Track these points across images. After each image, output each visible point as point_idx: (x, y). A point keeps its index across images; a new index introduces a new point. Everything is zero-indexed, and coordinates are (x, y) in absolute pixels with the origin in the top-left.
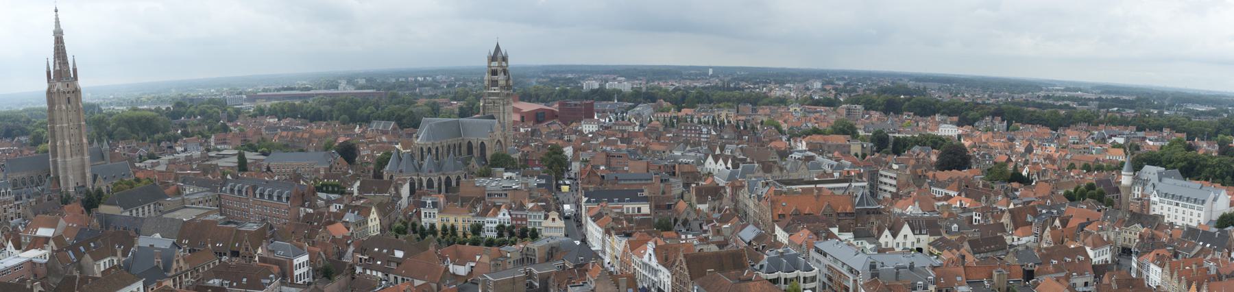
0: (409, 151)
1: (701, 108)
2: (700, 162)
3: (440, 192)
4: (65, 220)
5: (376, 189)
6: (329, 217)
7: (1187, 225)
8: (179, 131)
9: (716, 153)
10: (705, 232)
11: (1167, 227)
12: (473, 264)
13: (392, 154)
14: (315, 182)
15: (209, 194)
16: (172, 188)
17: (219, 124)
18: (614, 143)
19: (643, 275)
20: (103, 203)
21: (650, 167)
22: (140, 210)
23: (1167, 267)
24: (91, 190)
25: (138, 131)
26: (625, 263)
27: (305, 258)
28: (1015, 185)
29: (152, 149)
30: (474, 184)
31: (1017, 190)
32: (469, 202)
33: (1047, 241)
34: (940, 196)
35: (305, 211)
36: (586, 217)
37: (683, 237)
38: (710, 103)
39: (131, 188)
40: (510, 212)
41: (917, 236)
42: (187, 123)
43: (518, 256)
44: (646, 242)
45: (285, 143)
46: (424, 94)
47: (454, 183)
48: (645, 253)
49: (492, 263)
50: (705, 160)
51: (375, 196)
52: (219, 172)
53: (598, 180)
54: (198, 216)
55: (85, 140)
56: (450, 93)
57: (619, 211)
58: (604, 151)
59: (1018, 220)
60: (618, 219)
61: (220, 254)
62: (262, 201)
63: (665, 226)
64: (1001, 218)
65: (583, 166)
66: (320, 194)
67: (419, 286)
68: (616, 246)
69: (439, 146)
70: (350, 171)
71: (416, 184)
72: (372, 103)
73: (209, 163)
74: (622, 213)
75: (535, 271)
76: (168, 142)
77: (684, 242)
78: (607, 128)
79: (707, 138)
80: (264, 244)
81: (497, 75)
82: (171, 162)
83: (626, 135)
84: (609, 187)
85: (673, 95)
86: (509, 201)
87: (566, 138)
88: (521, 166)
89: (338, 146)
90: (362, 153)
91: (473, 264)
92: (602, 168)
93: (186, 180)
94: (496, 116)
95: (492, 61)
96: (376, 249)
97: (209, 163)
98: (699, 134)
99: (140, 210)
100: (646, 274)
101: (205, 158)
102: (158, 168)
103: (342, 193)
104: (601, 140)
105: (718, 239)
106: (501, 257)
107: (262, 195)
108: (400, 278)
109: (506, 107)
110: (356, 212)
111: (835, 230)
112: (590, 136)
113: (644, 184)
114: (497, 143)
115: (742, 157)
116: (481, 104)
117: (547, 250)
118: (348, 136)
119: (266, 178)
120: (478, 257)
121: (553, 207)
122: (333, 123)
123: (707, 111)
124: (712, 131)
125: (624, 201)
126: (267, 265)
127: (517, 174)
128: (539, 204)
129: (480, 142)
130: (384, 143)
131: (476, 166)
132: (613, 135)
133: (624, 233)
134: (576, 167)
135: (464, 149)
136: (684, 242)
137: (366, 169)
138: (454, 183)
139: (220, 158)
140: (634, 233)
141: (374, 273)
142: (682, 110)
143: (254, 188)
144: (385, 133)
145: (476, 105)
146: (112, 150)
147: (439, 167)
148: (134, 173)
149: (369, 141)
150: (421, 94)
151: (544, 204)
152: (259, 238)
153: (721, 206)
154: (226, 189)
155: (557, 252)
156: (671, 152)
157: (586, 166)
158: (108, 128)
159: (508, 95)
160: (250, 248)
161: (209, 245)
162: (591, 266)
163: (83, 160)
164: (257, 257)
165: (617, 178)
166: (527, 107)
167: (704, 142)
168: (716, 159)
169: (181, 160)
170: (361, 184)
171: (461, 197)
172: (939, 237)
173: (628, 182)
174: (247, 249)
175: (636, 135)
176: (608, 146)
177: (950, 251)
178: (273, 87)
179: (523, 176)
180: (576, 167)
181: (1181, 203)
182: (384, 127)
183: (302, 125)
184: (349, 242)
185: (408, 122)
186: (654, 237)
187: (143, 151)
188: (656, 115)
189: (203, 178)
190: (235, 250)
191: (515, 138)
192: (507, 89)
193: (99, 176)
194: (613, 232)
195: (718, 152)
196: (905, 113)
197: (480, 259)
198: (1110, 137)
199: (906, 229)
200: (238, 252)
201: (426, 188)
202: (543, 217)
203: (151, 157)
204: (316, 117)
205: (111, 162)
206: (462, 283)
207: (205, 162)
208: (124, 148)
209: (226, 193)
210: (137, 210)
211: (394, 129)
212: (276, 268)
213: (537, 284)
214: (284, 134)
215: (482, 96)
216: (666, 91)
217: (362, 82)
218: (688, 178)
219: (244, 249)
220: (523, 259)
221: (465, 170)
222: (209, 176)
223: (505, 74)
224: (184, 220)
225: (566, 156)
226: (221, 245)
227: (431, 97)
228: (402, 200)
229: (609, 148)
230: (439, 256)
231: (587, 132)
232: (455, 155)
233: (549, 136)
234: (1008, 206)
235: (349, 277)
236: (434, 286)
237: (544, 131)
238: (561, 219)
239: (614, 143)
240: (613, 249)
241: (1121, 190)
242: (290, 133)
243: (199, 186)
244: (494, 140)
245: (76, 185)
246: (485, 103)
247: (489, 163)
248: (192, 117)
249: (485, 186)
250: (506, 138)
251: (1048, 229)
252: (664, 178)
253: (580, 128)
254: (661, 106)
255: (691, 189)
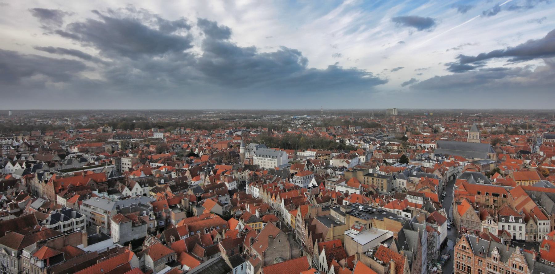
7: (270, 168)
11: (261, 170)
23: (261, 188)
28: (192, 157)
31: (193, 160)
33: (208, 182)
34: (155, 167)
41: (143, 188)
59: (194, 174)
64: (185, 173)
111: (96, 192)
115: (33, 160)
168: (14, 164)
172: (154, 187)
177: (160, 193)
181: (266, 159)
195: (15, 159)
196: (135, 129)
198: (235, 133)
199: (137, 185)
234: (189, 168)
241: (240, 155)
251: (208, 176)
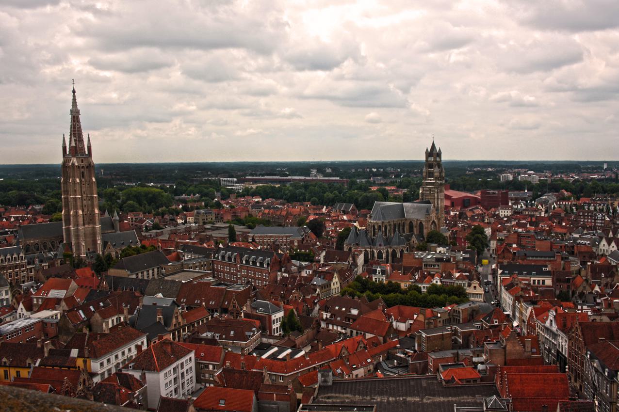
0: (365, 228)
1: (597, 198)
2: (595, 244)
3: (387, 262)
4: (75, 282)
5: (338, 259)
6: (300, 280)
8: (181, 206)
9: (610, 236)
10: (598, 304)
12: (412, 322)
13: (350, 231)
14: (290, 251)
15: (203, 260)
16: (174, 254)
17: (214, 201)
18: (523, 226)
19: (546, 338)
20: (112, 267)
21: (554, 247)
22: (145, 273)
24: (101, 255)
25: (145, 204)
26: (531, 326)
27: (280, 314)
29: (157, 220)
30: (414, 256)
32: (409, 271)
35: (282, 275)
36: (500, 286)
37: (579, 307)
38: (605, 193)
39: (137, 254)
40: (441, 280)
42: (188, 200)
43: (446, 317)
44: (548, 310)
45: (267, 219)
46: (377, 182)
47: (398, 255)
48: (547, 319)
49: (426, 321)
50: (599, 243)
51: (337, 264)
52: (213, 242)
53: (511, 256)
54: (195, 279)
55: (97, 211)
56: (397, 182)
57: (527, 282)
58: (516, 232)
60: (526, 289)
61: (212, 311)
62: (247, 267)
63: (564, 297)
65: (499, 244)
66: (293, 261)
67: (369, 339)
68: (523, 312)
69: (388, 224)
70: (318, 243)
71: (369, 255)
72: (336, 188)
73: (205, 234)
74: (529, 285)
75: (460, 330)
76: (171, 216)
77: (580, 312)
78: (519, 213)
79: (601, 223)
80: (248, 303)
81: (433, 168)
82: (173, 233)
83: (534, 219)
84: (520, 261)
85: (574, 186)
86: (440, 271)
87: (486, 221)
88: (451, 243)
89: (309, 223)
90: (328, 229)
91: (412, 322)
92: (514, 246)
93: (186, 248)
94: (431, 201)
95: (430, 157)
96: (337, 308)
97: (205, 234)
98: (595, 219)
99: (145, 273)
100: (548, 337)
101: (202, 229)
102: (160, 238)
103: (312, 261)
104: (513, 223)
105: (609, 311)
106: (433, 317)
107: (247, 262)
108: (355, 332)
109: (439, 194)
110: (322, 277)
112: (505, 219)
113: (548, 261)
114: (432, 223)
116: (420, 192)
117: (469, 312)
118: (317, 214)
119: (251, 248)
120: (415, 316)
121: (475, 277)
122: (306, 203)
123: (602, 200)
124: (606, 217)
125: (531, 274)
126: (250, 320)
127: (447, 249)
128: (464, 274)
129: (419, 222)
130: (345, 221)
131: (416, 242)
132: (524, 219)
133: (530, 301)
134: (493, 244)
135: (407, 228)
136: (580, 312)
137: (330, 242)
138: (398, 255)
139: (214, 230)
140: (539, 301)
141: (335, 328)
142: (581, 199)
143: (241, 256)
144: (345, 213)
145: (416, 193)
146: (121, 221)
147: (388, 242)
148: (141, 241)
149: (333, 219)
150: (374, 181)
151: (468, 274)
152: (243, 297)
153: (613, 283)
154: (218, 256)
155: (476, 314)
156: (571, 234)
157: (502, 244)
158: (118, 201)
159: (441, 184)
160: (237, 305)
161: (204, 303)
162: (503, 327)
163: (94, 229)
164: (243, 314)
165: (525, 254)
166: (456, 194)
167: (599, 226)
169: (181, 231)
170: (326, 254)
171: (404, 267)
173: (535, 258)
174: (234, 307)
175: (542, 219)
176: (519, 228)
178: (258, 173)
179: (452, 251)
180: (493, 244)
182: (345, 208)
183: (280, 204)
184: (316, 301)
185: (365, 205)
186: (554, 306)
187: (148, 222)
188: (558, 203)
189: (200, 246)
190: (225, 307)
191: (446, 220)
192: (441, 180)
193: (109, 243)
194: (522, 300)
197: (417, 317)
200: (228, 309)
201: (376, 259)
202: (466, 285)
203: (156, 227)
204: (292, 198)
205: (120, 231)
206: (403, 337)
207: (201, 232)
208: (132, 219)
209: (218, 259)
210: (143, 273)
211: (353, 210)
212: (258, 323)
213: (461, 341)
214: (267, 211)
215: (421, 185)
216: (567, 182)
217: (329, 170)
218: (585, 257)
219: (232, 308)
220: (450, 319)
221: (407, 245)
222: (205, 245)
223: (439, 168)
224: (183, 281)
225: (486, 236)
226: (213, 303)
227: (382, 184)
228: (358, 268)
229: (520, 230)
230: (385, 314)
231: (503, 216)
232: (400, 233)
233: (472, 218)
235: (315, 331)
236: (381, 339)
237: (469, 214)
238: (480, 287)
239: (525, 224)
240: (521, 313)
242: (272, 211)
243: (196, 253)
244: (430, 221)
245: (88, 252)
246: (423, 190)
247: (426, 240)
248: (192, 195)
249: (422, 259)
250: (439, 219)
252: (564, 256)
253: (497, 213)
254: (563, 194)
255: (587, 267)
